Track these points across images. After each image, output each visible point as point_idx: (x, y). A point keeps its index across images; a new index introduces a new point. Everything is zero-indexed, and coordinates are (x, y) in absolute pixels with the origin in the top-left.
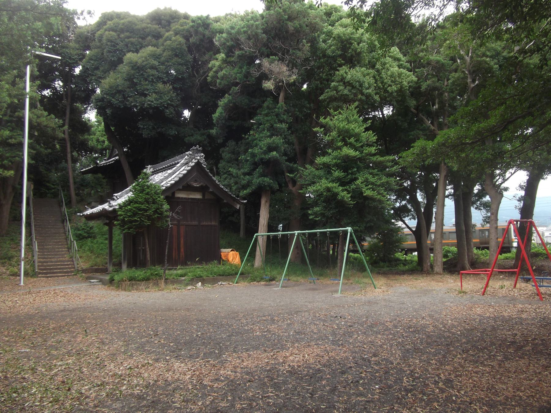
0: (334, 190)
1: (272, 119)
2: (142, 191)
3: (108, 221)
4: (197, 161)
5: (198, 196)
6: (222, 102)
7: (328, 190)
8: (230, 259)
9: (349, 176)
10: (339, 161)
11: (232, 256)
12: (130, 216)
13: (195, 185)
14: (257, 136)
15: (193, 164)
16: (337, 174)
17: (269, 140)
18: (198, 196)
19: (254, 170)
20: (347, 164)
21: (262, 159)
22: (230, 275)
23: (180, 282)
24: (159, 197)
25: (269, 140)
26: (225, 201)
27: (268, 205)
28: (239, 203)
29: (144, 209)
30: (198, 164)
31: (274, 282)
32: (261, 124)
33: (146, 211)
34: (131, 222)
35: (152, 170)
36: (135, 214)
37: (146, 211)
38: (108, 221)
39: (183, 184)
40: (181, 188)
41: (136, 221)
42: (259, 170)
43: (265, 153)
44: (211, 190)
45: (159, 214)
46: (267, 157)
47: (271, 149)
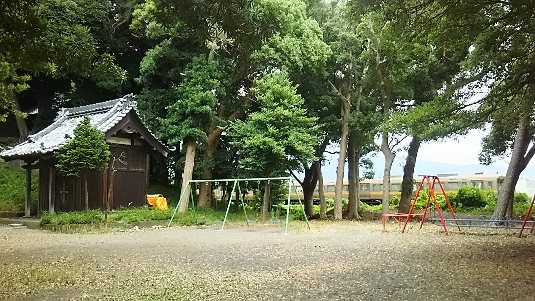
0: (270, 144)
1: (205, 74)
2: (87, 135)
3: (26, 164)
4: (131, 108)
5: (128, 143)
6: (151, 53)
7: (264, 143)
8: (159, 205)
9: (282, 133)
10: (273, 119)
11: (159, 201)
12: (75, 160)
13: (129, 131)
14: (187, 89)
15: (128, 111)
16: (272, 130)
17: (201, 94)
18: (128, 143)
19: (183, 120)
20: (279, 122)
21: (194, 111)
22: (162, 219)
23: (116, 225)
24: (102, 142)
25: (201, 94)
26: (155, 149)
27: (194, 153)
28: (167, 152)
29: (90, 153)
30: (132, 111)
31: (204, 226)
32: (192, 78)
33: (92, 155)
34: (76, 165)
35: (68, 113)
36: (81, 158)
37: (92, 155)
38: (26, 164)
39: (117, 131)
40: (115, 133)
41: (82, 165)
42: (189, 120)
43: (197, 105)
44: (142, 137)
45: (103, 159)
46: (199, 109)
47: (204, 102)
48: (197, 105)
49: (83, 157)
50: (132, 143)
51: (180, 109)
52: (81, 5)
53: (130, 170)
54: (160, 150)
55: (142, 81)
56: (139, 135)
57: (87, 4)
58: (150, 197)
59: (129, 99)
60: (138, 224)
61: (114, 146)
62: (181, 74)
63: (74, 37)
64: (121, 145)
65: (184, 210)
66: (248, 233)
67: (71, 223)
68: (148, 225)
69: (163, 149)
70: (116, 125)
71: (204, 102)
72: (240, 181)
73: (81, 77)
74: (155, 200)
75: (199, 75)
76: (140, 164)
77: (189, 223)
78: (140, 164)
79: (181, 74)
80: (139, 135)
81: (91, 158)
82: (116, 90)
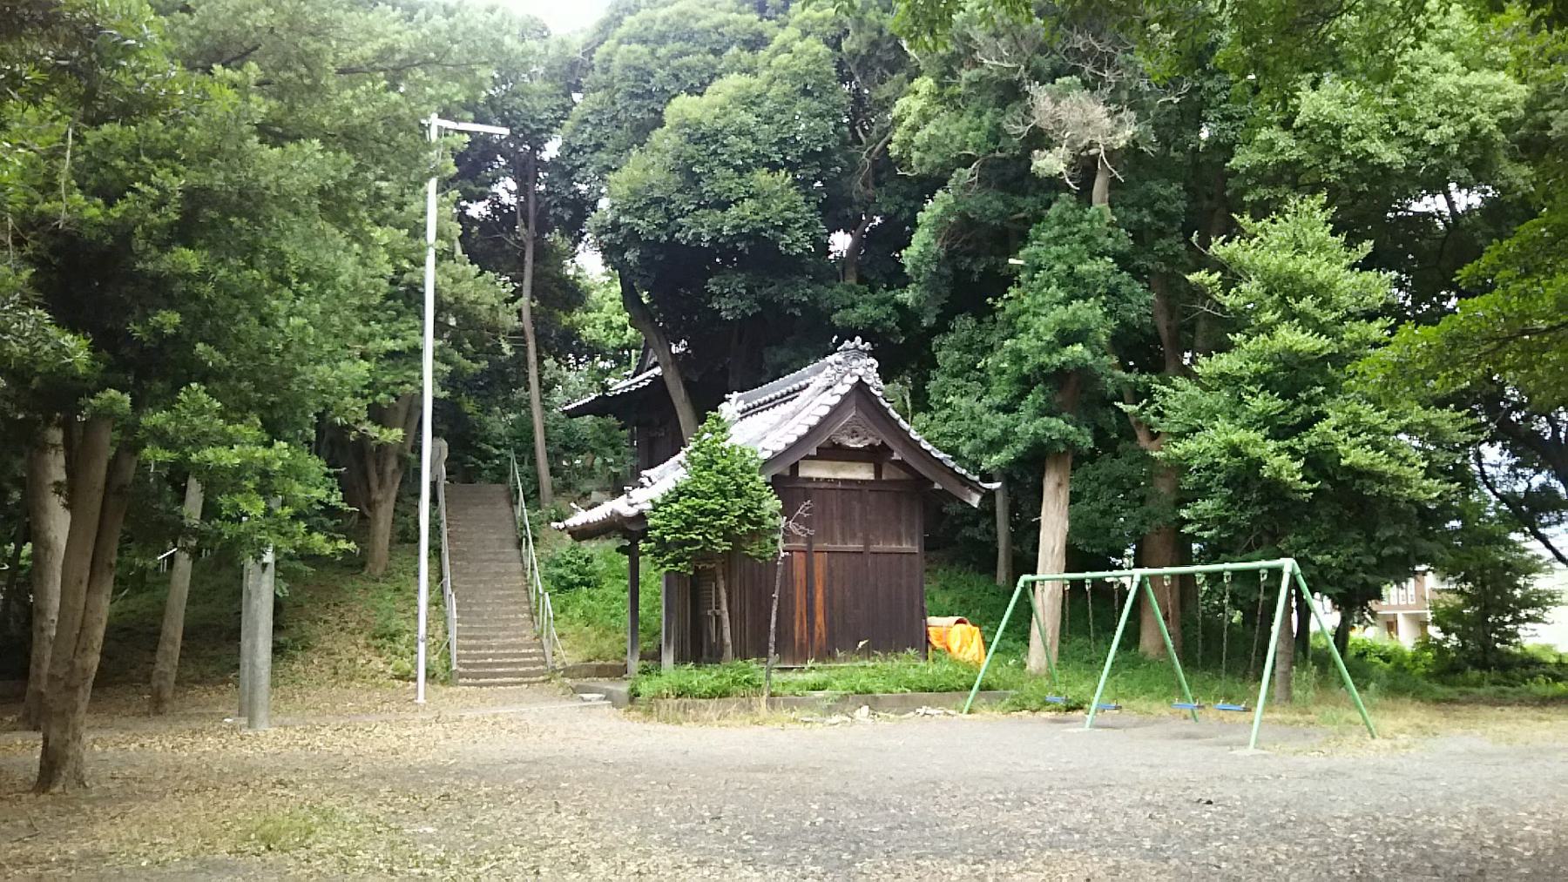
0: (1250, 450)
1: (1074, 251)
2: (709, 464)
3: (628, 543)
4: (856, 379)
5: (864, 473)
6: (932, 209)
7: (1234, 450)
8: (954, 647)
9: (1300, 410)
10: (1266, 367)
11: (957, 637)
12: (677, 531)
13: (852, 443)
14: (1027, 301)
15: (847, 388)
16: (1260, 403)
17: (1062, 313)
18: (864, 473)
19: (1021, 396)
20: (1294, 378)
21: (1041, 367)
22: (949, 690)
23: (811, 706)
24: (753, 479)
25: (1062, 313)
26: (937, 486)
27: (1064, 496)
28: (978, 492)
29: (713, 511)
30: (861, 387)
31: (1080, 713)
32: (1039, 268)
33: (719, 515)
34: (681, 544)
35: (742, 406)
36: (689, 525)
37: (719, 515)
38: (628, 543)
39: (823, 443)
40: (814, 452)
41: (694, 542)
42: (1036, 397)
43: (1051, 349)
44: (896, 456)
45: (751, 522)
46: (1056, 360)
47: (1066, 337)
48: (1051, 349)
49: (695, 522)
50: (878, 472)
51: (1013, 362)
52: (769, 120)
53: (875, 547)
54: (955, 488)
55: (918, 301)
56: (885, 450)
57: (782, 112)
58: (938, 624)
59: (851, 354)
60: (875, 704)
61: (823, 485)
62: (1011, 261)
63: (749, 203)
64: (844, 481)
65: (1044, 663)
66: (1180, 742)
67: (678, 696)
68: (904, 705)
69: (964, 485)
70: (812, 429)
71: (1066, 337)
72: (1152, 577)
73: (793, 304)
74: (947, 632)
75: (1058, 257)
76: (903, 530)
77: (1034, 704)
78: (903, 530)
79: (1011, 261)
80: (885, 450)
81: (717, 523)
82: (884, 329)
